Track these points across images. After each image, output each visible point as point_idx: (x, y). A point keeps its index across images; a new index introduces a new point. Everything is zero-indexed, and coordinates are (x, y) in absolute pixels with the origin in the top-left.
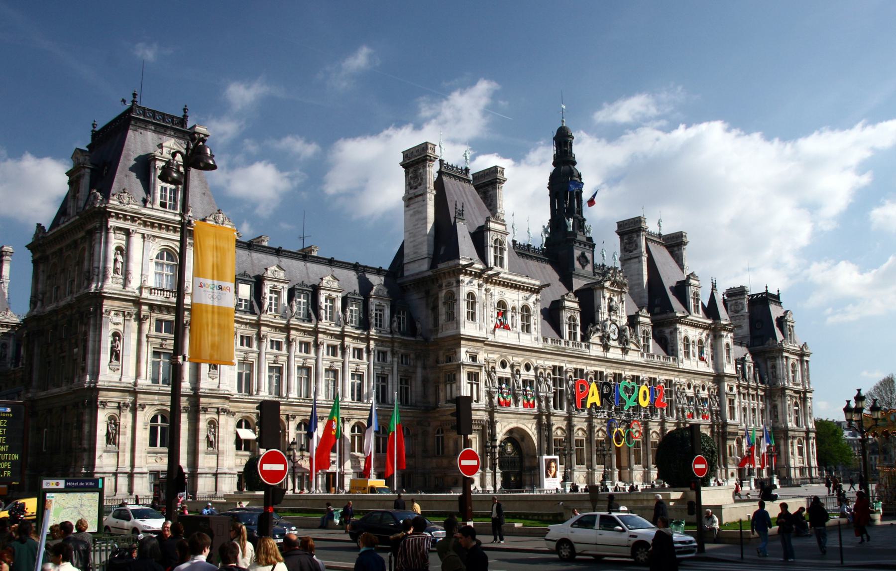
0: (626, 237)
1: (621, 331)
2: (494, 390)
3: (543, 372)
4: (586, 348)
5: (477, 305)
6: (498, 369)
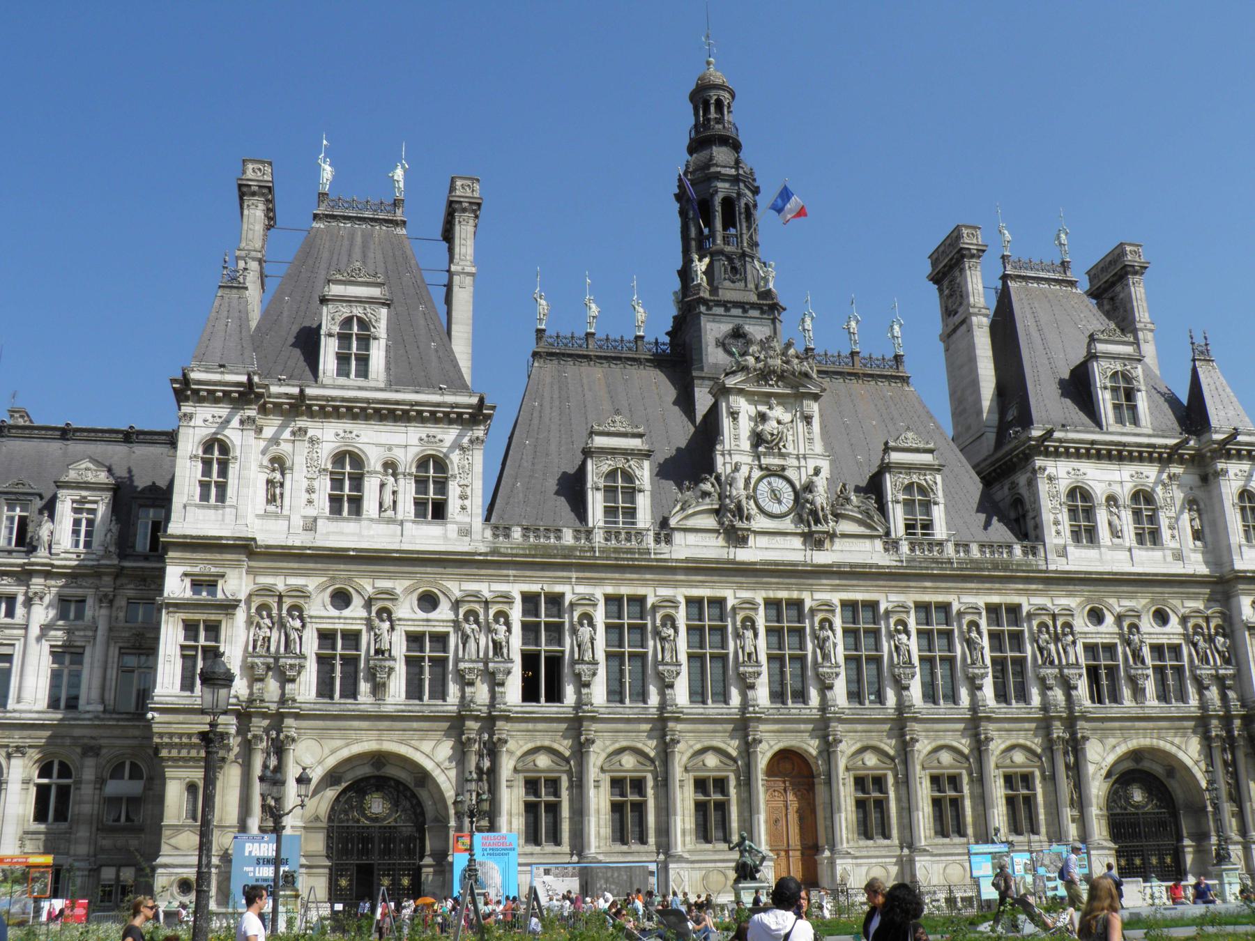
0: (946, 283)
1: (802, 494)
2: (290, 661)
3: (481, 612)
4: (657, 541)
5: (233, 470)
6: (320, 609)
